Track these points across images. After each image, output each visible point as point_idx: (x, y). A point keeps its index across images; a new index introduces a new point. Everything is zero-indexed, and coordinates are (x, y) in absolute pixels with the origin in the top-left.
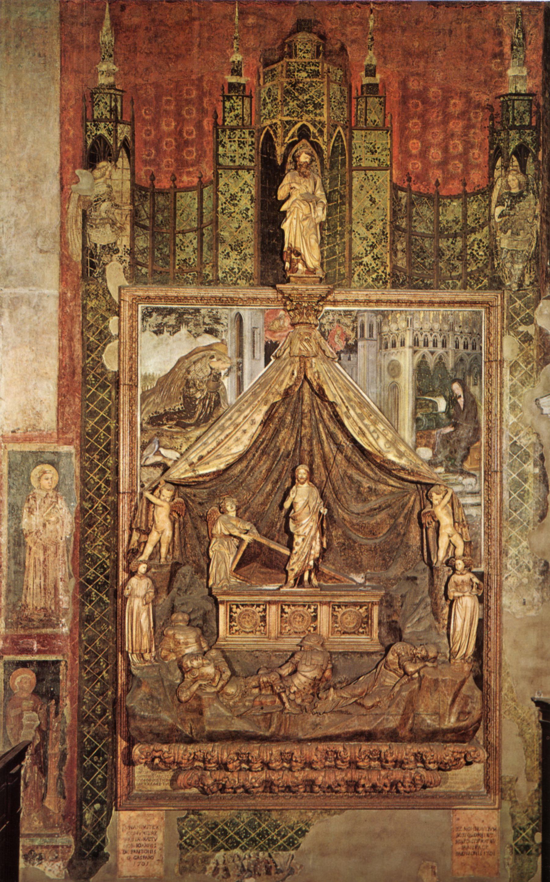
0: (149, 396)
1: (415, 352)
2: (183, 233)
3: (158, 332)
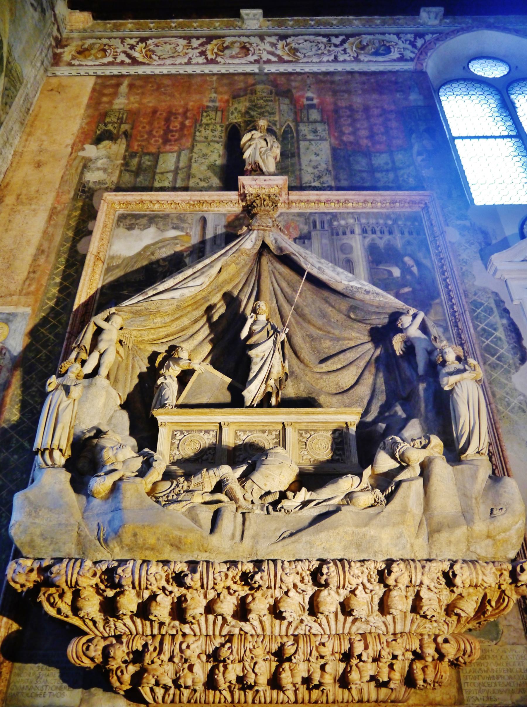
0: (113, 270)
1: (365, 237)
2: (162, 173)
3: (130, 228)
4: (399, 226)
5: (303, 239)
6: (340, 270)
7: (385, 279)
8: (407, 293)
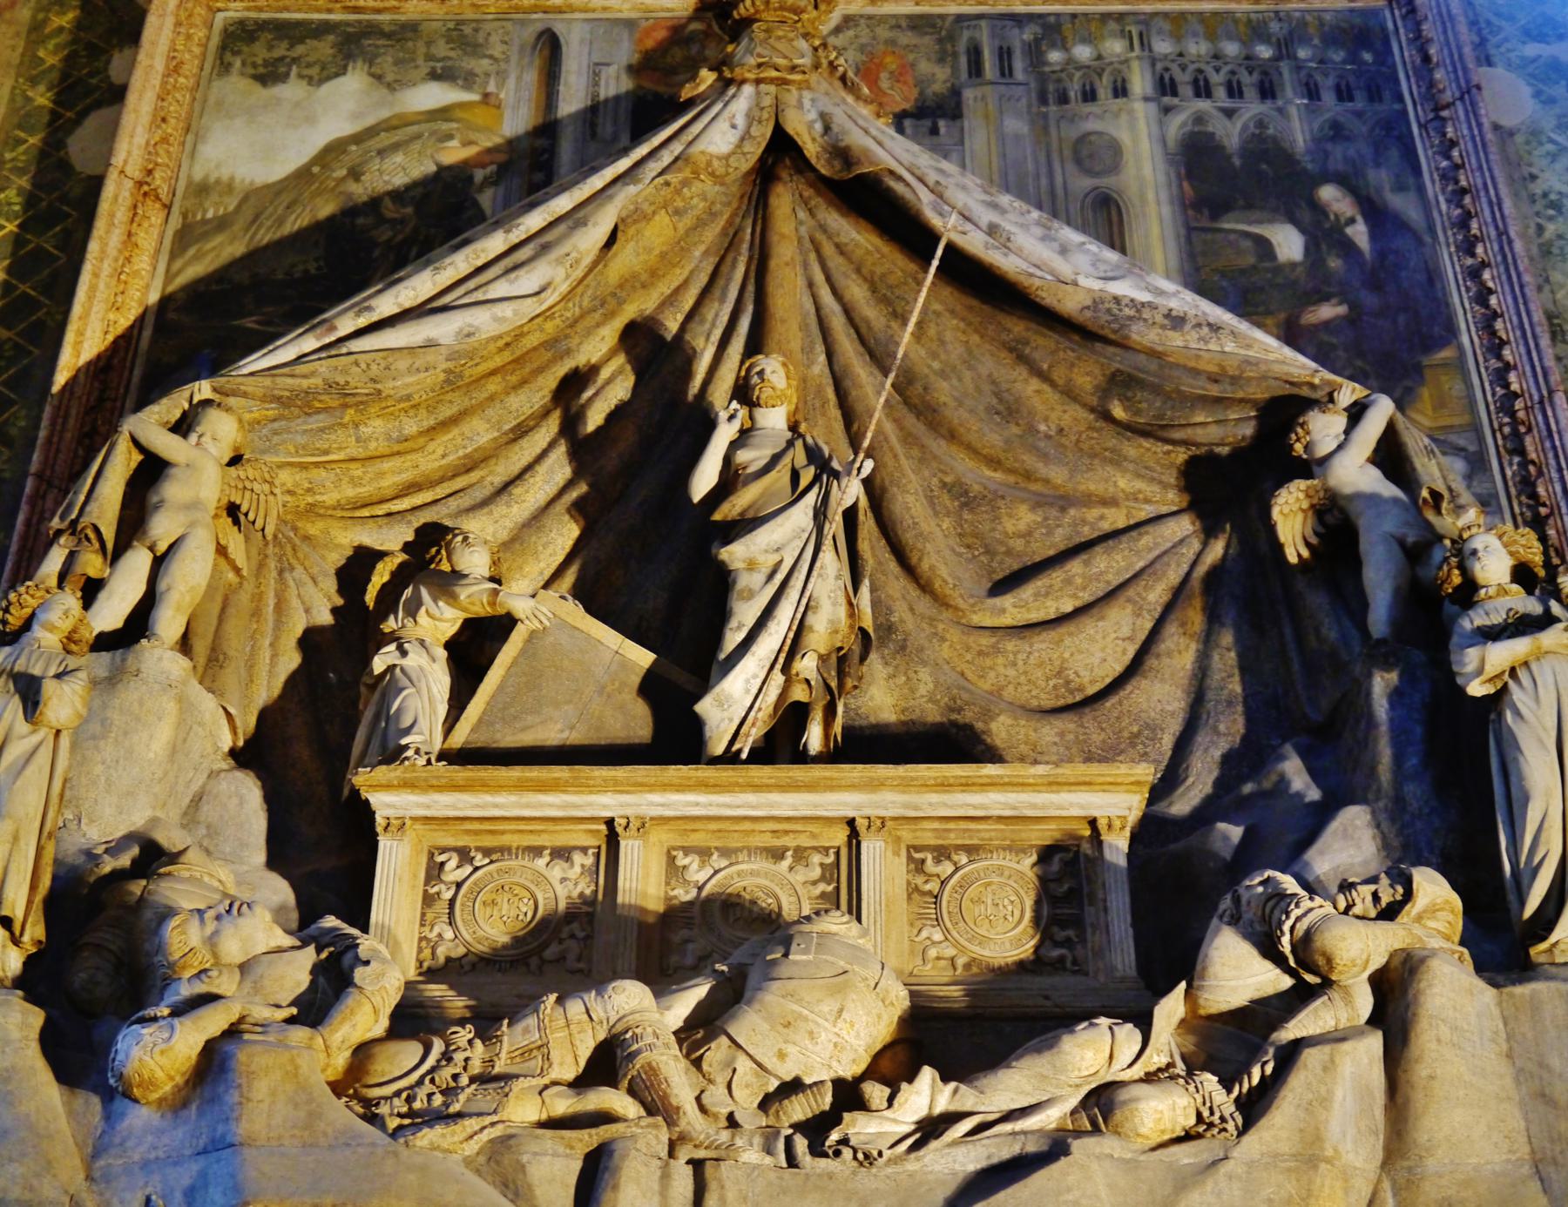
0: (205, 236)
1: (1167, 110)
3: (269, 76)
4: (1298, 67)
5: (931, 117)
6: (1072, 236)
7: (1243, 272)
8: (1326, 325)
